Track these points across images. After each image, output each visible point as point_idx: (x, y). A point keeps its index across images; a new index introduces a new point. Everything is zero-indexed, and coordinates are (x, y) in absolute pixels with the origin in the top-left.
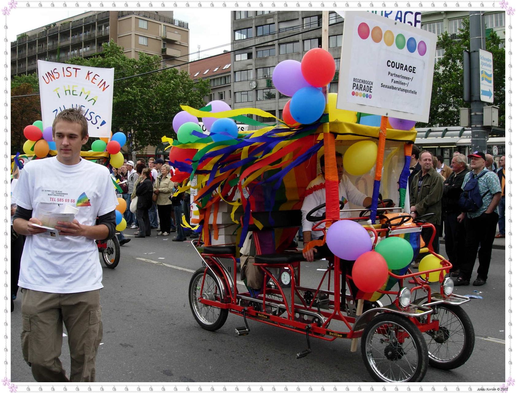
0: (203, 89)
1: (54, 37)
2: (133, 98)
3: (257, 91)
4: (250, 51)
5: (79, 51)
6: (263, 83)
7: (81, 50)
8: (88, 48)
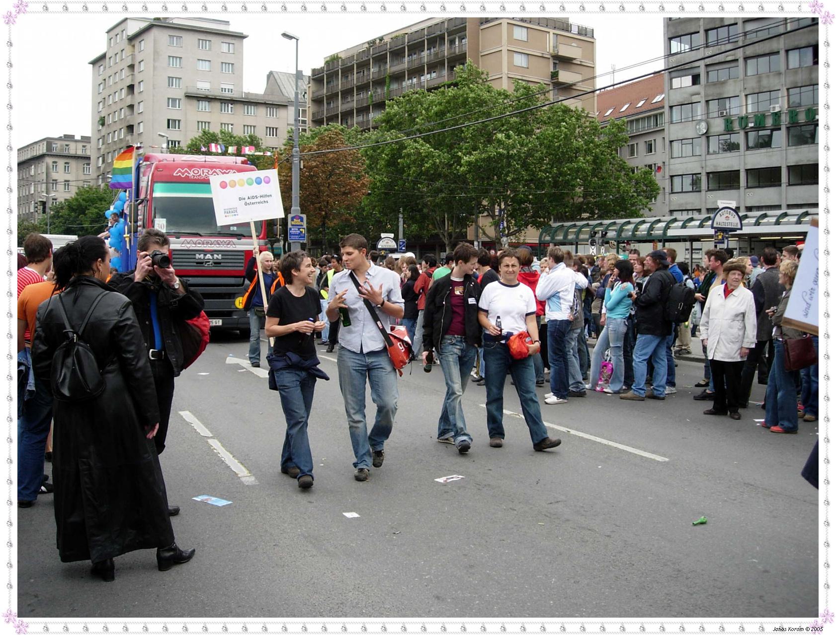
1: (380, 59)
2: (505, 152)
3: (708, 137)
4: (695, 71)
5: (420, 79)
6: (718, 125)
7: (422, 78)
8: (434, 75)
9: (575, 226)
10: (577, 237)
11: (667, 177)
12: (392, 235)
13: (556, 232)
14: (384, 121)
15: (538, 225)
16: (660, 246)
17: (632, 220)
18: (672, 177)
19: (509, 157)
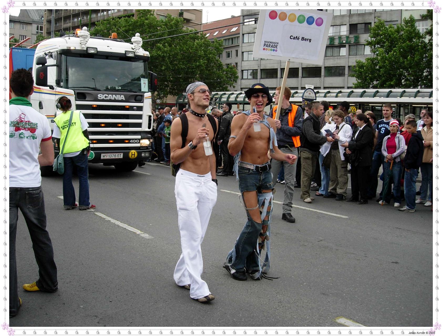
0: (218, 48)
11: (240, 71)
16: (241, 107)
17: (227, 93)
18: (242, 71)
19: (164, 57)
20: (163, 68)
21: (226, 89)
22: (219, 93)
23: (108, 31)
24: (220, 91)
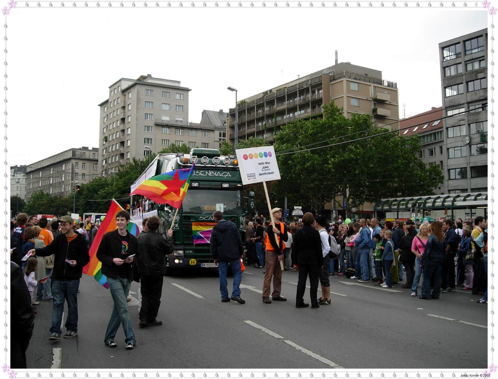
1: (271, 103)
5: (294, 114)
7: (296, 113)
8: (303, 112)
9: (396, 201)
10: (398, 207)
12: (301, 208)
13: (384, 204)
14: (279, 139)
15: (371, 201)
16: (449, 212)
17: (432, 196)
18: (449, 170)
19: (357, 160)
20: (357, 172)
21: (430, 192)
22: (423, 197)
23: (295, 135)
24: (424, 195)
